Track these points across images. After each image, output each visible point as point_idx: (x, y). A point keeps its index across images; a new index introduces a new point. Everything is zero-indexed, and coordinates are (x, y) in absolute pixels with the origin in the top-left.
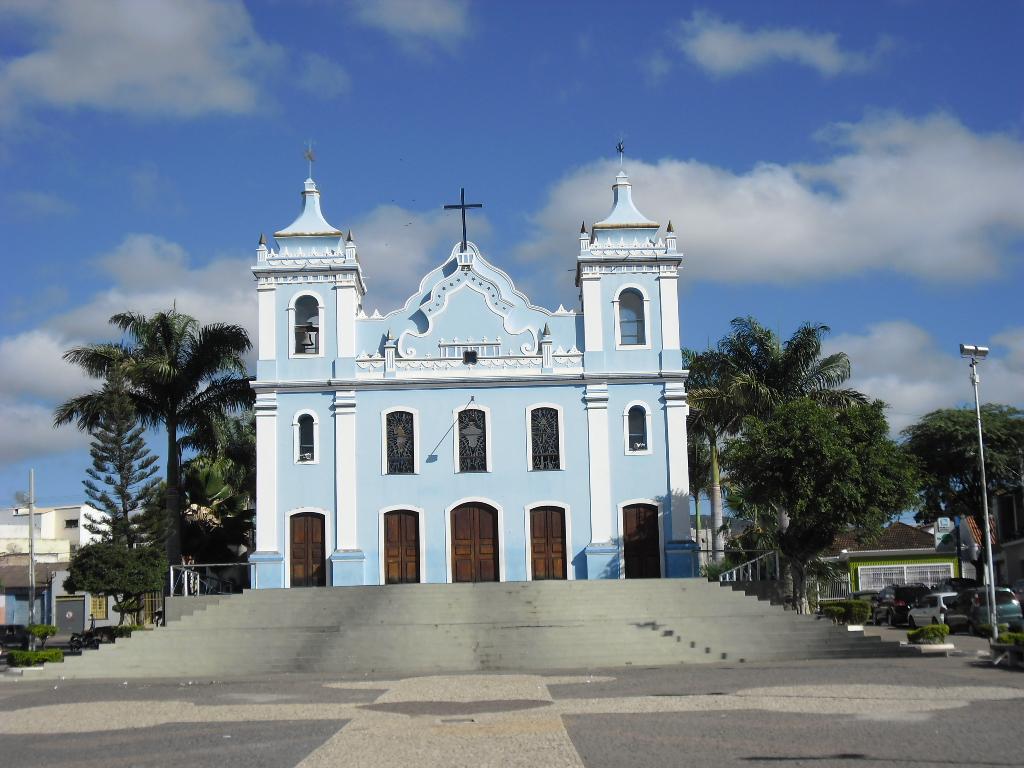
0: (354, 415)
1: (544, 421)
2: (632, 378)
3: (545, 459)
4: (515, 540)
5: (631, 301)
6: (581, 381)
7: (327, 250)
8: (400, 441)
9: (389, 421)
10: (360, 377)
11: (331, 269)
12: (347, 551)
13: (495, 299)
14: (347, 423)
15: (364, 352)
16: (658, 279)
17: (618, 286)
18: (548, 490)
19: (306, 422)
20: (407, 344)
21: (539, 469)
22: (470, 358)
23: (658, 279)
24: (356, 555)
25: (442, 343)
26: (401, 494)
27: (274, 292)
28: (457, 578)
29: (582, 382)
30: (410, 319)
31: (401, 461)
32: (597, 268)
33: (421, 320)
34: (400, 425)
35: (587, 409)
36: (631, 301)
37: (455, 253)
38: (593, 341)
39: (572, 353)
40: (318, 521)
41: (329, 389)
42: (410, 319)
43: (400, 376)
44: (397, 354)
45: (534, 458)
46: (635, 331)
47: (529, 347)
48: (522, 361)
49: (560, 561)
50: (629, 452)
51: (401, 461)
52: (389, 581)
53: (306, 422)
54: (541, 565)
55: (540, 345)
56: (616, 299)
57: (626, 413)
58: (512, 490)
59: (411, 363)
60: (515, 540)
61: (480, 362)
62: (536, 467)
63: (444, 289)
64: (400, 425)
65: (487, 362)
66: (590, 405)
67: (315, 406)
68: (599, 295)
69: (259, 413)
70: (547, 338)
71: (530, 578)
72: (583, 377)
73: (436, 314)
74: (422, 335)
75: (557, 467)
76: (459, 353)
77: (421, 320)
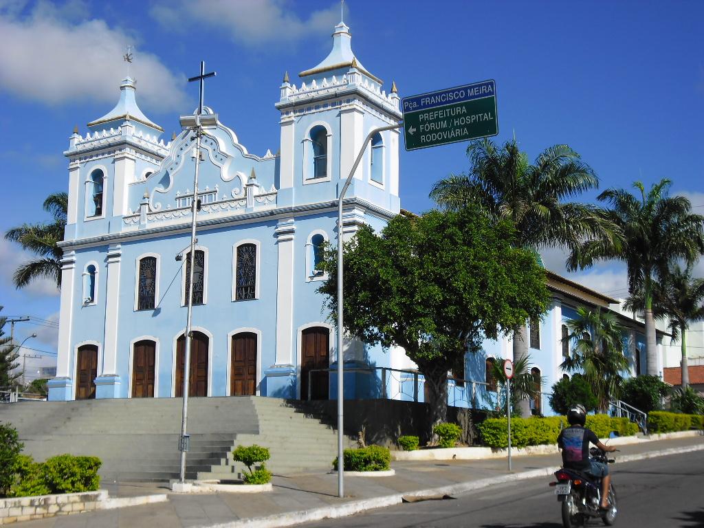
0: (119, 263)
1: (246, 256)
2: (313, 208)
3: (246, 290)
4: (220, 359)
5: (319, 136)
6: (269, 219)
7: (140, 134)
8: (148, 281)
9: (141, 266)
10: (125, 230)
12: (106, 376)
13: (216, 153)
14: (115, 269)
16: (339, 115)
17: (309, 124)
18: (246, 318)
19: (92, 269)
20: (155, 201)
21: (241, 298)
23: (339, 115)
24: (110, 381)
25: (178, 196)
26: (145, 327)
27: (78, 169)
28: (134, 395)
29: (271, 218)
31: (147, 301)
32: (292, 114)
34: (148, 265)
35: (277, 243)
36: (319, 136)
38: (287, 180)
39: (271, 192)
41: (102, 245)
44: (150, 210)
45: (238, 289)
47: (237, 190)
48: (233, 204)
49: (253, 382)
50: (309, 280)
51: (147, 301)
52: (78, 398)
53: (92, 269)
54: (239, 383)
55: (245, 189)
56: (307, 136)
57: (309, 241)
58: (221, 321)
59: (159, 216)
60: (220, 359)
61: (204, 208)
62: (240, 298)
63: (181, 149)
64: (148, 265)
66: (281, 237)
67: (95, 259)
68: (293, 137)
69: (64, 267)
70: (254, 181)
71: (130, 395)
72: (272, 213)
74: (167, 190)
75: (253, 297)
76: (188, 202)
77: (165, 180)
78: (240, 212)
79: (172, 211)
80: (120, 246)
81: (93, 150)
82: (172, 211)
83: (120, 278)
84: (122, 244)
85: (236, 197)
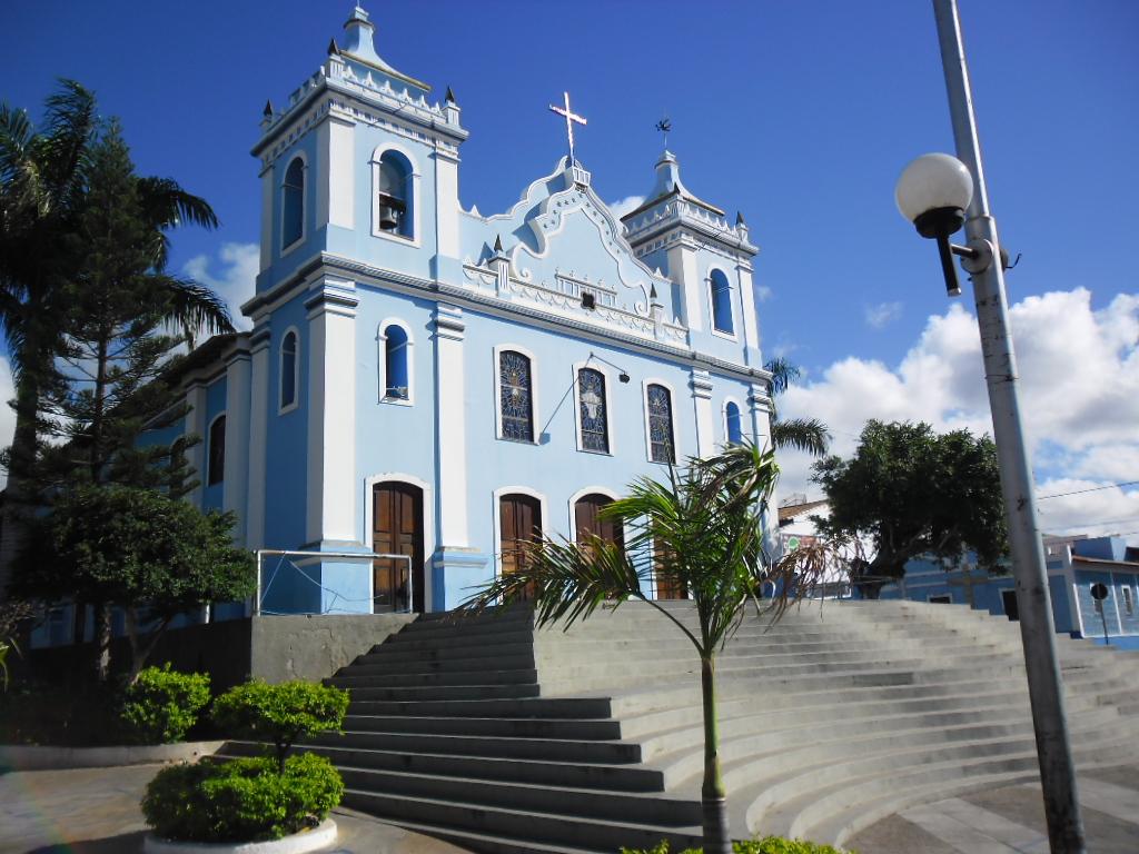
11: (432, 127)
15: (468, 257)
19: (395, 338)
22: (588, 302)
26: (521, 470)
27: (352, 129)
29: (689, 363)
30: (514, 233)
31: (519, 423)
33: (529, 235)
34: (516, 366)
35: (694, 396)
37: (560, 169)
40: (408, 500)
42: (514, 233)
43: (517, 301)
46: (722, 320)
51: (519, 423)
61: (598, 309)
64: (516, 366)
65: (604, 313)
66: (698, 391)
67: (412, 320)
73: (553, 233)
77: (529, 235)
78: (647, 336)
79: (552, 293)
80: (458, 311)
81: (394, 113)
82: (552, 293)
83: (461, 369)
84: (463, 310)
85: (641, 314)
